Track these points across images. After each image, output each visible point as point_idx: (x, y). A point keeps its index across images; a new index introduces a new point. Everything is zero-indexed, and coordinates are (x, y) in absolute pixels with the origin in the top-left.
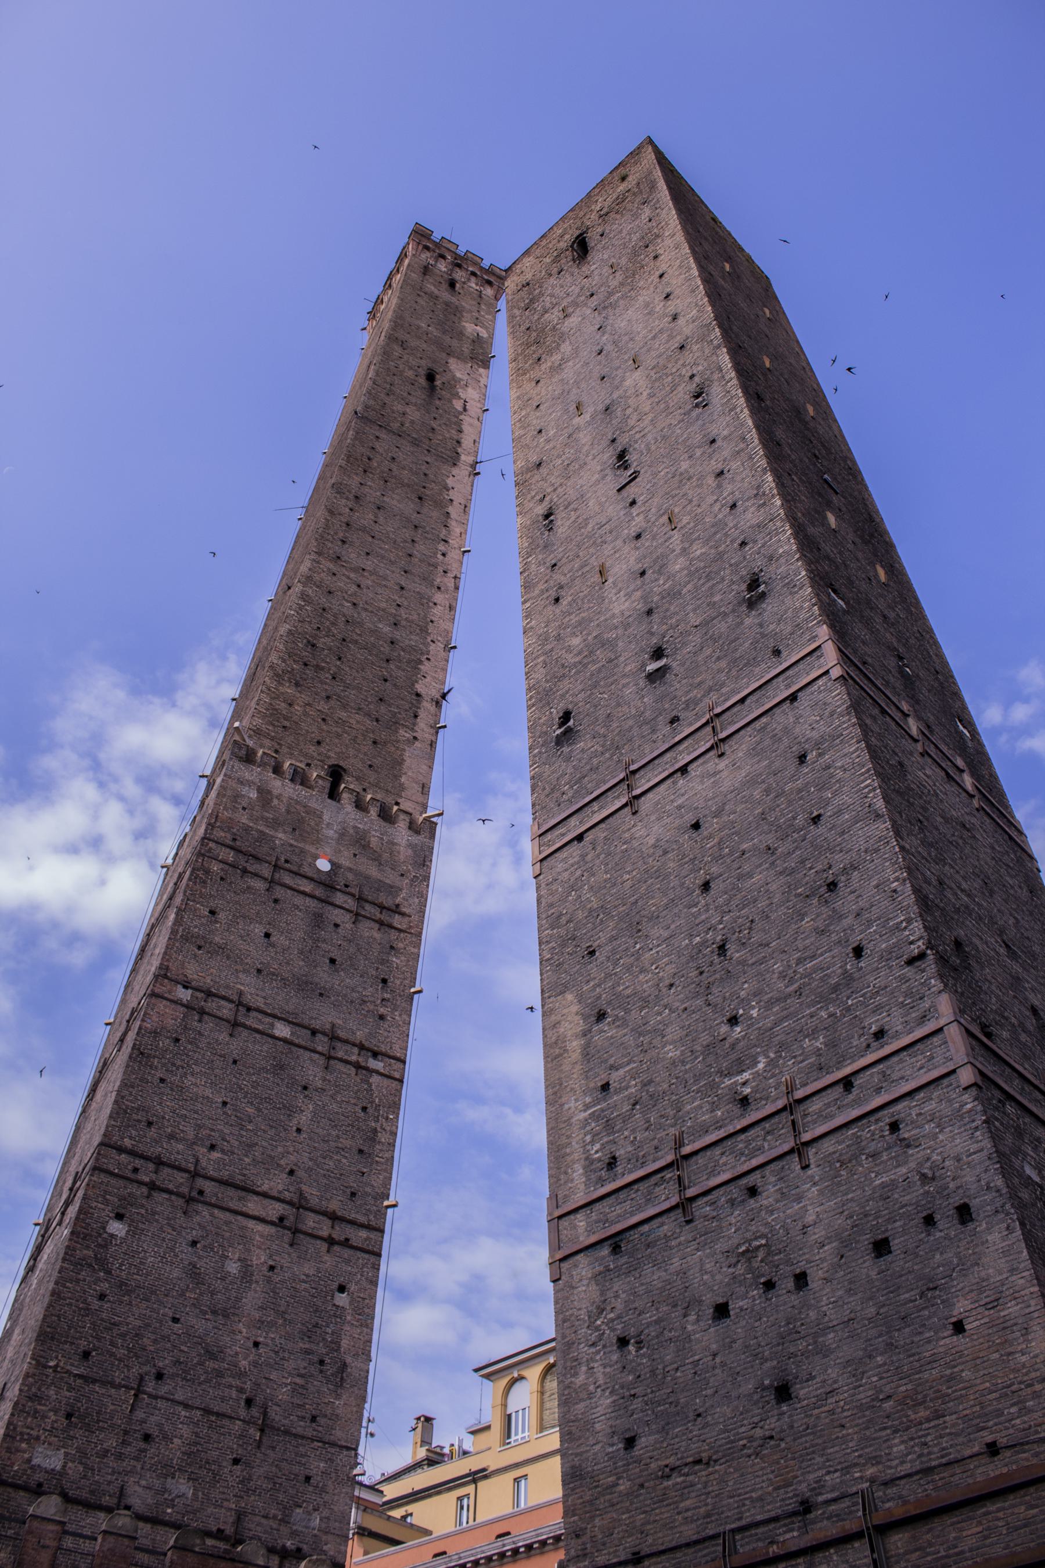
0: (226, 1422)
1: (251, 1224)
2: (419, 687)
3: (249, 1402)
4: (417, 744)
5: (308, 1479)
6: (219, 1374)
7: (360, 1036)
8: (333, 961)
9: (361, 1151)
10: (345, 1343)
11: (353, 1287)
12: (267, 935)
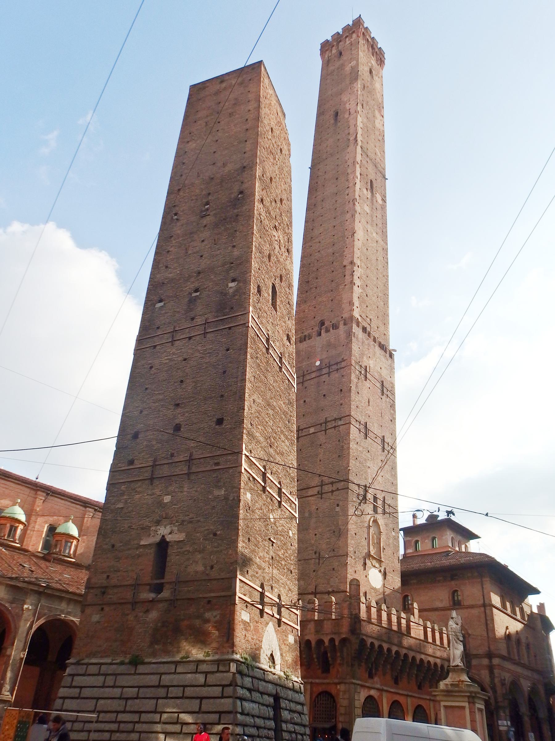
0: (310, 561)
1: (310, 498)
2: (344, 263)
3: (315, 553)
4: (346, 287)
5: (334, 569)
6: (307, 548)
7: (335, 416)
8: (324, 395)
9: (339, 456)
10: (340, 523)
11: (340, 503)
12: (305, 401)
